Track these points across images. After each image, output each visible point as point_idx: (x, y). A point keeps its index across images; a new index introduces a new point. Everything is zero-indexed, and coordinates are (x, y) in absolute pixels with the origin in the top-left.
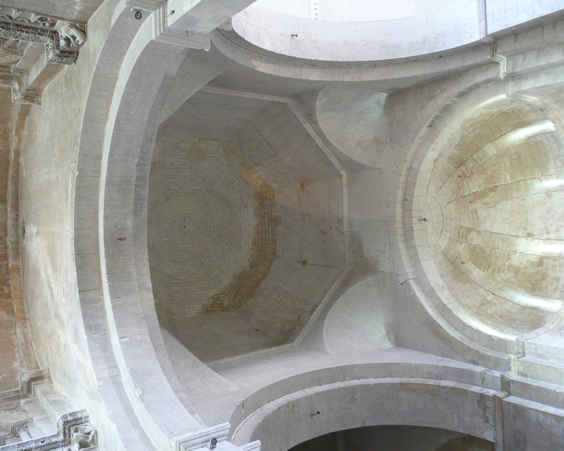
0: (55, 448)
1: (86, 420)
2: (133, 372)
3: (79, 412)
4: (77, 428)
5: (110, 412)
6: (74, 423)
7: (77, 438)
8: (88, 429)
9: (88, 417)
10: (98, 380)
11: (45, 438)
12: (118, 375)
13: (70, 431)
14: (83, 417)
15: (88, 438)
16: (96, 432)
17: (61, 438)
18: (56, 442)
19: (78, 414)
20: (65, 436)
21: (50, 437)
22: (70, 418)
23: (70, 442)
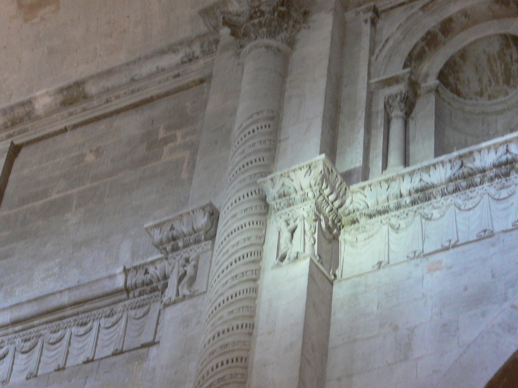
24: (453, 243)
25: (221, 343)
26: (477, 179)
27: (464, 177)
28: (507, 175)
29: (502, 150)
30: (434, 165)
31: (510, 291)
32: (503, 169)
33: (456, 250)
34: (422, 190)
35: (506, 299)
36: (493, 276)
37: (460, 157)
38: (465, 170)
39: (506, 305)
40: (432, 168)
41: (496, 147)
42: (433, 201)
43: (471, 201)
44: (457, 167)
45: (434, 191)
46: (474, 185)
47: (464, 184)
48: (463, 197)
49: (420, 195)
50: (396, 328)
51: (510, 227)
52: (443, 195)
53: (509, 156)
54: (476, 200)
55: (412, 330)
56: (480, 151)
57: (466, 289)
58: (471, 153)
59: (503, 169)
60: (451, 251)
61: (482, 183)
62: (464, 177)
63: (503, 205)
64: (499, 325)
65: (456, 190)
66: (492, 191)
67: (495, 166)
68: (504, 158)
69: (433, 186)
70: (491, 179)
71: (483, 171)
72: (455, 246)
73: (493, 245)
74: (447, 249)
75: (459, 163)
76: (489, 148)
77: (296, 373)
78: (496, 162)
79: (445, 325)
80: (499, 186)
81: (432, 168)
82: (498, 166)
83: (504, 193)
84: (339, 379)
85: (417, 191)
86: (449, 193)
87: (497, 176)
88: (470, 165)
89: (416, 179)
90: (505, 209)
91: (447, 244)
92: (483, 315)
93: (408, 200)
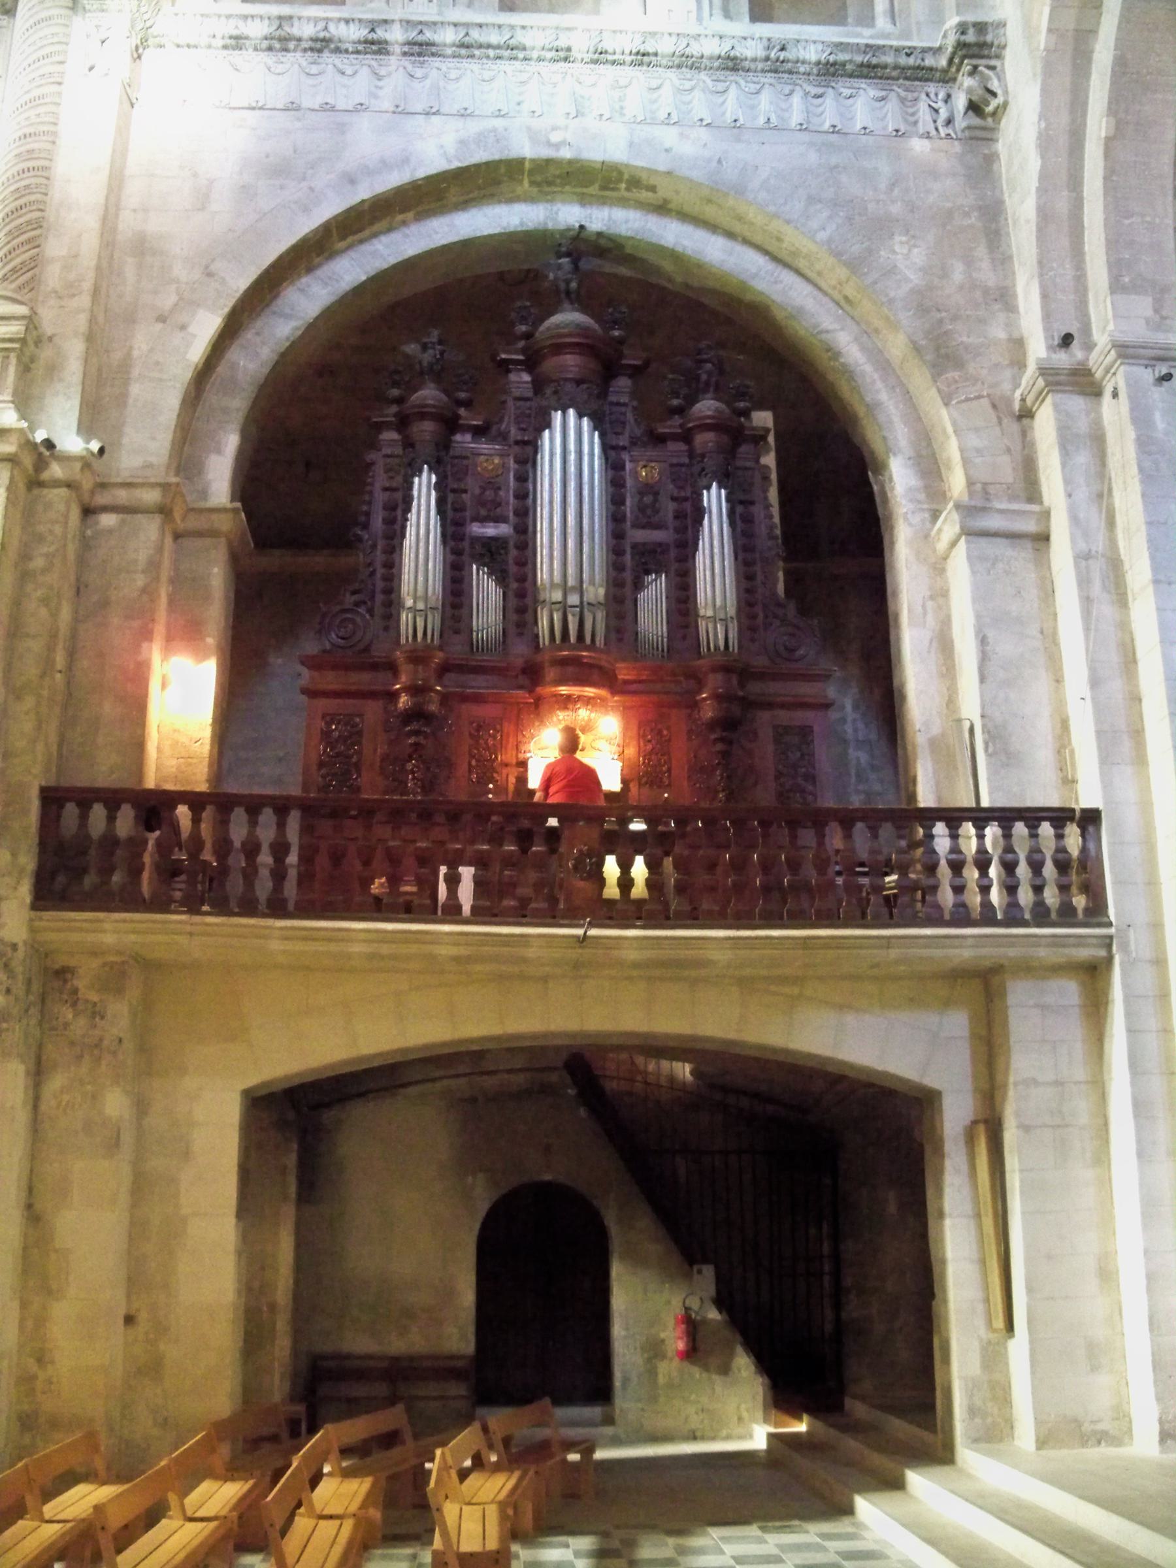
0: (927, 80)
1: (998, 51)
2: (1121, 65)
3: (992, 24)
4: (975, 67)
5: (1043, 125)
6: (975, 50)
7: (970, 91)
8: (994, 85)
9: (1004, 47)
10: (1050, 30)
11: (915, 48)
12: (1094, 32)
13: (961, 63)
14: (996, 43)
15: (988, 104)
16: (1005, 105)
17: (943, 62)
18: (931, 69)
19: (990, 29)
20: (951, 61)
21: (924, 50)
22: (971, 37)
23: (954, 80)
24: (260, 104)
25: (28, 147)
26: (291, 45)
27: (280, 39)
28: (320, 51)
29: (321, 25)
30: (252, 17)
31: (310, 171)
32: (318, 45)
33: (261, 112)
34: (237, 38)
35: (304, 179)
36: (295, 152)
37: (280, 18)
38: (283, 33)
39: (304, 184)
40: (250, 19)
41: (316, 20)
42: (243, 52)
43: (281, 66)
44: (275, 27)
45: (247, 43)
46: (286, 50)
47: (277, 45)
48: (274, 59)
49: (233, 42)
50: (195, 175)
51: (317, 107)
52: (256, 49)
53: (327, 35)
54: (288, 66)
55: (211, 182)
56: (300, 18)
57: (267, 156)
58: (291, 18)
59: (318, 45)
60: (257, 112)
61: (295, 50)
62: (280, 39)
63: (311, 81)
64: (296, 202)
65: (270, 49)
66: (304, 63)
67: (311, 39)
68: (322, 35)
69: (247, 38)
70: (305, 50)
71: (299, 40)
72: (261, 108)
73: (299, 119)
74: (253, 108)
75: (277, 23)
76: (309, 19)
77: (103, 201)
78: (313, 35)
79: (243, 187)
80: (310, 60)
81: (250, 19)
82: (315, 40)
83: (314, 69)
84: (135, 211)
85: (231, 37)
86: (261, 50)
87: (312, 49)
88: (287, 28)
89: (233, 22)
90: (314, 86)
91: (254, 105)
92: (282, 188)
93: (220, 43)
